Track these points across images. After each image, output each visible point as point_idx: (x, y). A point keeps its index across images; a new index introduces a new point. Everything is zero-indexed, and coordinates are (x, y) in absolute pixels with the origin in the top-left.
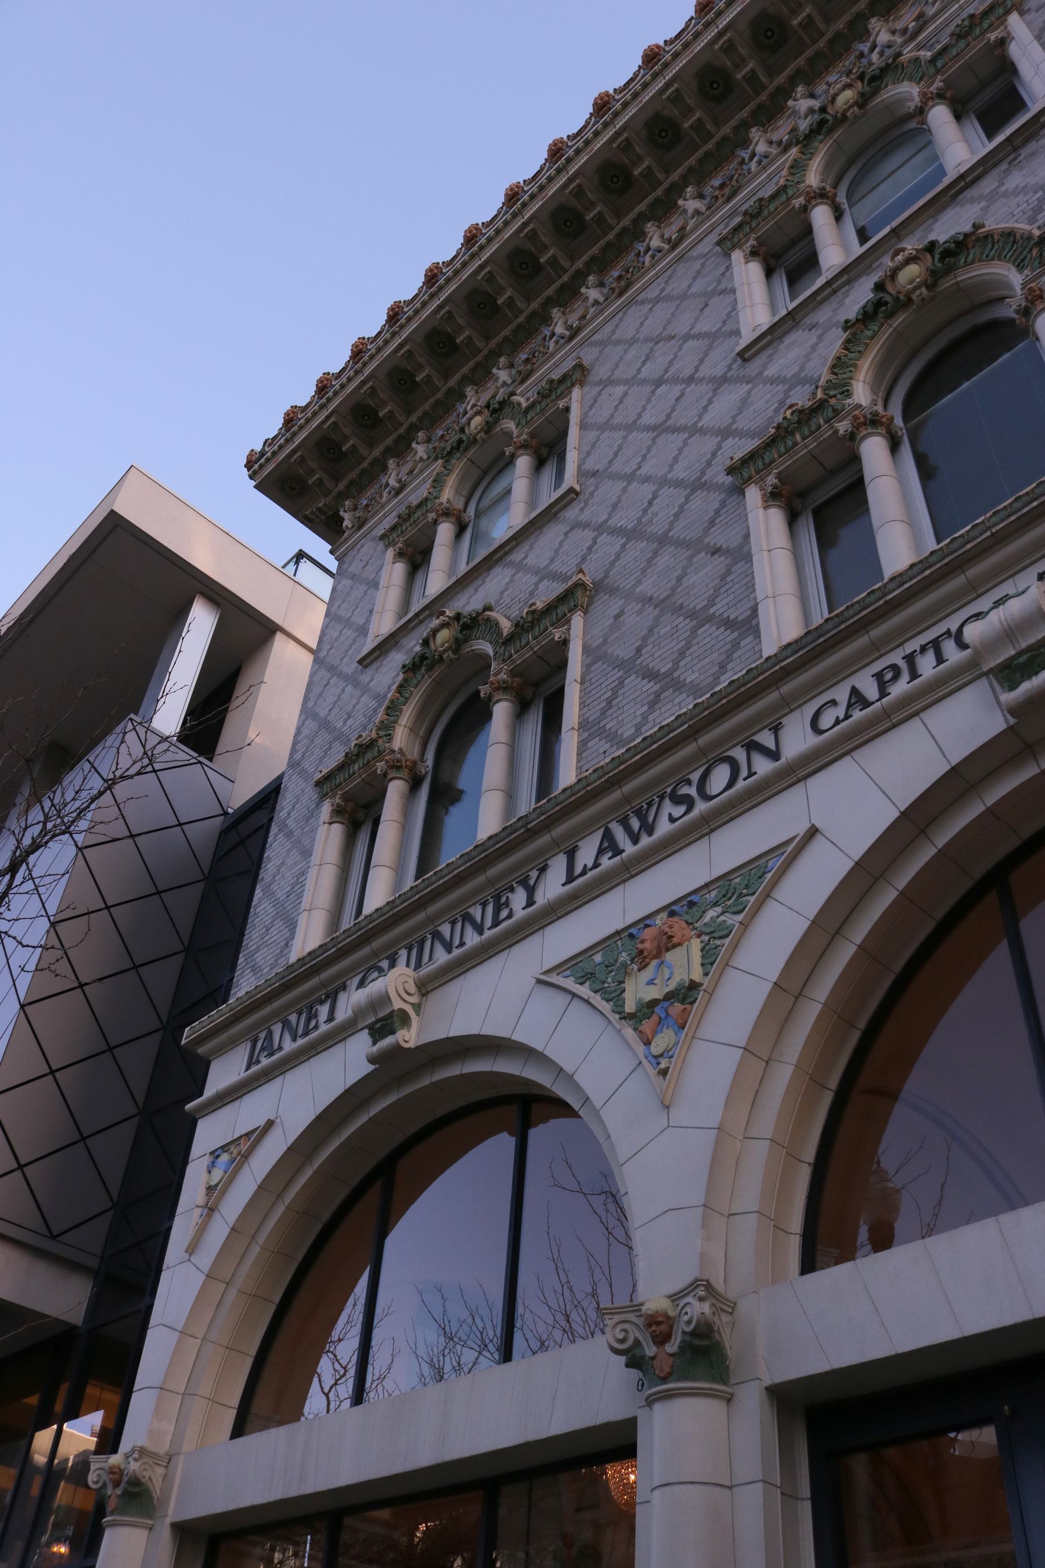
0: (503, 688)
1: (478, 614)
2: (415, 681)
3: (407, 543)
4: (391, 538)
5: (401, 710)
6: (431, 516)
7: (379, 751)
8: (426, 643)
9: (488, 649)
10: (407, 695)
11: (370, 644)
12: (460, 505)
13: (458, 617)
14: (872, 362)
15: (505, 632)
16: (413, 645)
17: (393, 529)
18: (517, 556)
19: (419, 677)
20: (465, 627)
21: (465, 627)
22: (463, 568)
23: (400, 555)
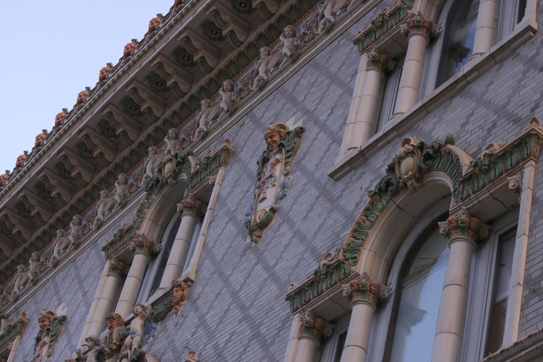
0: (460, 227)
1: (440, 146)
2: (380, 206)
3: (380, 51)
5: (367, 234)
6: (403, 27)
8: (391, 169)
9: (448, 182)
10: (372, 219)
11: (340, 160)
12: (432, 18)
13: (421, 146)
14: (378, 233)
15: (465, 170)
16: (380, 163)
17: (368, 34)
18: (478, 88)
19: (384, 202)
20: (428, 157)
21: (428, 157)
22: (431, 92)
23: (374, 62)
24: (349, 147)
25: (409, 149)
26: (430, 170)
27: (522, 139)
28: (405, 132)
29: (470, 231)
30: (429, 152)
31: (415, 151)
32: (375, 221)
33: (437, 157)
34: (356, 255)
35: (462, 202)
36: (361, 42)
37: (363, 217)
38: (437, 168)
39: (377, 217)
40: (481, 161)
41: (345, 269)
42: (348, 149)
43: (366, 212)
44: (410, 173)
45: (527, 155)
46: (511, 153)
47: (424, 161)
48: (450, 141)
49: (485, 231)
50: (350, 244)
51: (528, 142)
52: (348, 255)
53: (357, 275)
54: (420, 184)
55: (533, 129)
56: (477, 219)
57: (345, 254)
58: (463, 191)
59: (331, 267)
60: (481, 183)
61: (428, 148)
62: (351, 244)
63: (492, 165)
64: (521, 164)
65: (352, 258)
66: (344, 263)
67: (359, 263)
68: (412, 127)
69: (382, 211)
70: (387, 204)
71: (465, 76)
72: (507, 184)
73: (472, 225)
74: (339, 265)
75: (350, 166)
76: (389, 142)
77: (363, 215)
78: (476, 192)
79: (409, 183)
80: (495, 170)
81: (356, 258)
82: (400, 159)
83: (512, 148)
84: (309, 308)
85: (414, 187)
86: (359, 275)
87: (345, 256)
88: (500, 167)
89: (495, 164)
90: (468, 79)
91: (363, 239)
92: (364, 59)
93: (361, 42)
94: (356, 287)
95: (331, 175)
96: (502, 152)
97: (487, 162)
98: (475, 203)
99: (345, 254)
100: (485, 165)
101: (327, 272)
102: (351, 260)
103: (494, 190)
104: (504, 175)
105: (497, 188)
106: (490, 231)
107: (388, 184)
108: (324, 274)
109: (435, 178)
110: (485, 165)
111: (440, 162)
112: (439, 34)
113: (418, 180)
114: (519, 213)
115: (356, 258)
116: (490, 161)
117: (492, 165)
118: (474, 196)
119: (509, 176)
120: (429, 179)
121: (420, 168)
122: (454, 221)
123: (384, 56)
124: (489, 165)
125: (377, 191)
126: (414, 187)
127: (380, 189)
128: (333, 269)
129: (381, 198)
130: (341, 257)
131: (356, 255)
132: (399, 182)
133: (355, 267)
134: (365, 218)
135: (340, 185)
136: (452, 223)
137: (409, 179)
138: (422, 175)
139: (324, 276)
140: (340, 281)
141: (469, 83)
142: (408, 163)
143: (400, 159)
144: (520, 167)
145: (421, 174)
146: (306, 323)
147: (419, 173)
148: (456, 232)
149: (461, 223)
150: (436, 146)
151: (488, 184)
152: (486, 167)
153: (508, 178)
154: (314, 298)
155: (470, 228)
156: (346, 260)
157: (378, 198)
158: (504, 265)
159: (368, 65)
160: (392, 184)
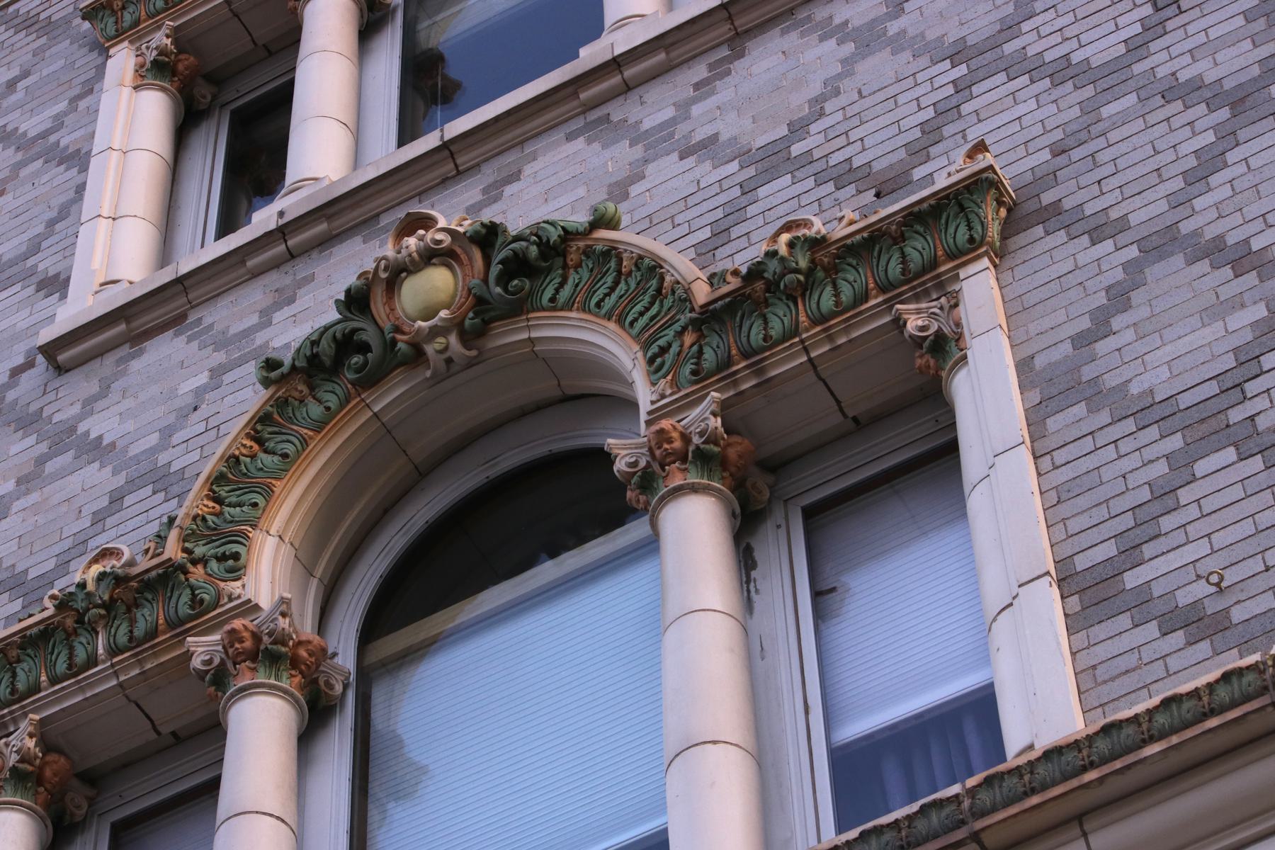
1: (568, 235)
4: (127, 18)
7: (196, 602)
20: (517, 266)
23: (158, 70)
24: (102, 280)
25: (440, 242)
26: (519, 308)
27: (947, 197)
28: (421, 194)
29: (41, 789)
30: (525, 251)
31: (459, 251)
32: (298, 454)
33: (549, 271)
34: (235, 548)
35: (696, 382)
36: (108, 12)
37: (248, 443)
38: (553, 300)
39: (305, 442)
40: (89, 595)
41: (193, 589)
42: (102, 285)
43: (259, 427)
44: (444, 314)
45: (971, 240)
46: (899, 239)
47: (504, 279)
48: (602, 221)
49: (77, 801)
50: (204, 519)
51: (967, 204)
52: (199, 551)
53: (250, 608)
54: (474, 353)
55: (991, 167)
56: (63, 760)
57: (187, 545)
58: (700, 352)
59: (134, 584)
60: (81, 655)
61: (518, 238)
62: (208, 517)
63: (820, 274)
64: (943, 269)
65: (222, 558)
66: (186, 572)
67: (251, 572)
68: (183, 317)
69: (319, 426)
70: (342, 406)
71: (616, 64)
72: (188, 655)
73: (48, 773)
74: (165, 579)
75: (128, 322)
76: (292, 255)
77: (248, 435)
78: (892, 286)
79: (430, 349)
80: (766, 322)
81: (236, 557)
82: (397, 273)
83: (900, 224)
84: (34, 711)
85: (449, 361)
86: (257, 608)
87: (185, 550)
88: (851, 280)
89: (832, 270)
90: (629, 72)
91: (255, 505)
92: (123, 60)
93: (108, 12)
94: (248, 644)
95: (50, 350)
96: (727, 300)
97: (803, 263)
98: (149, 666)
99: (187, 545)
100: (797, 271)
101: (112, 600)
102: (214, 565)
103: (79, 698)
104: (872, 302)
105: (162, 660)
106: (92, 801)
107: (346, 344)
108: (104, 605)
109: (534, 334)
110: (797, 271)
111: (562, 285)
112: (395, 10)
113: (466, 338)
114: (224, 745)
115: (236, 557)
116: (813, 261)
117: (820, 274)
118: (880, 299)
119: (901, 302)
120: (510, 335)
121: (480, 303)
122: (246, 634)
123: (192, 59)
124: (810, 273)
125: (301, 363)
126: (449, 361)
127: (313, 360)
128: (138, 591)
129: (312, 388)
130: (172, 550)
131: (235, 548)
132: (394, 342)
133: (238, 583)
134: (256, 447)
135: (81, 385)
136: (241, 641)
137: (435, 332)
138: (486, 323)
139: (103, 612)
140: (171, 625)
141: (628, 88)
142: (436, 283)
143: (397, 273)
144: (939, 276)
145: (479, 317)
146: (21, 761)
147: (476, 314)
148: (254, 670)
149: (275, 643)
150: (554, 235)
151: (164, 633)
152: (801, 278)
153: (899, 306)
154: (54, 681)
155: (40, 781)
156: (194, 562)
157: (301, 387)
158: (833, 590)
159: (140, 71)
160: (364, 348)
